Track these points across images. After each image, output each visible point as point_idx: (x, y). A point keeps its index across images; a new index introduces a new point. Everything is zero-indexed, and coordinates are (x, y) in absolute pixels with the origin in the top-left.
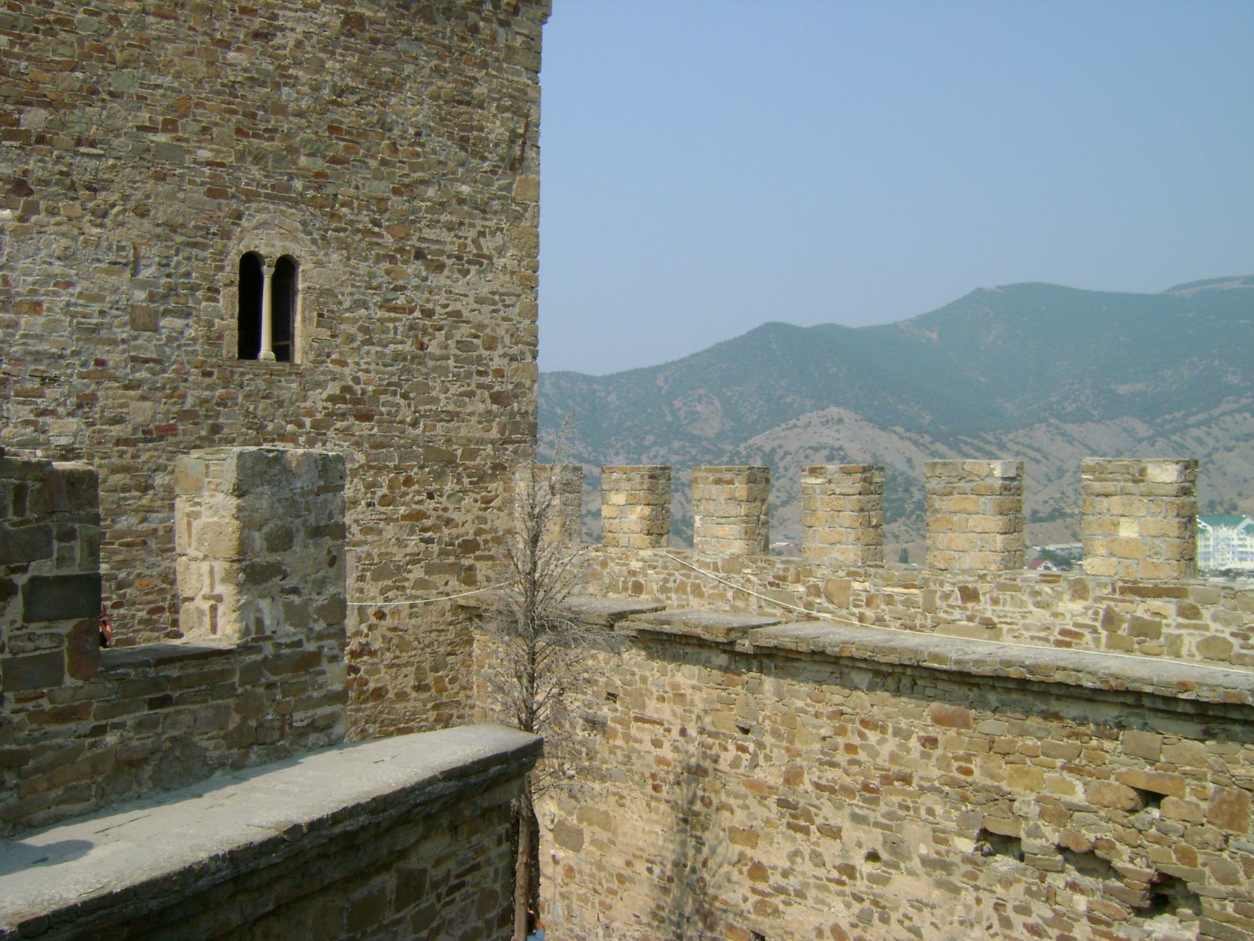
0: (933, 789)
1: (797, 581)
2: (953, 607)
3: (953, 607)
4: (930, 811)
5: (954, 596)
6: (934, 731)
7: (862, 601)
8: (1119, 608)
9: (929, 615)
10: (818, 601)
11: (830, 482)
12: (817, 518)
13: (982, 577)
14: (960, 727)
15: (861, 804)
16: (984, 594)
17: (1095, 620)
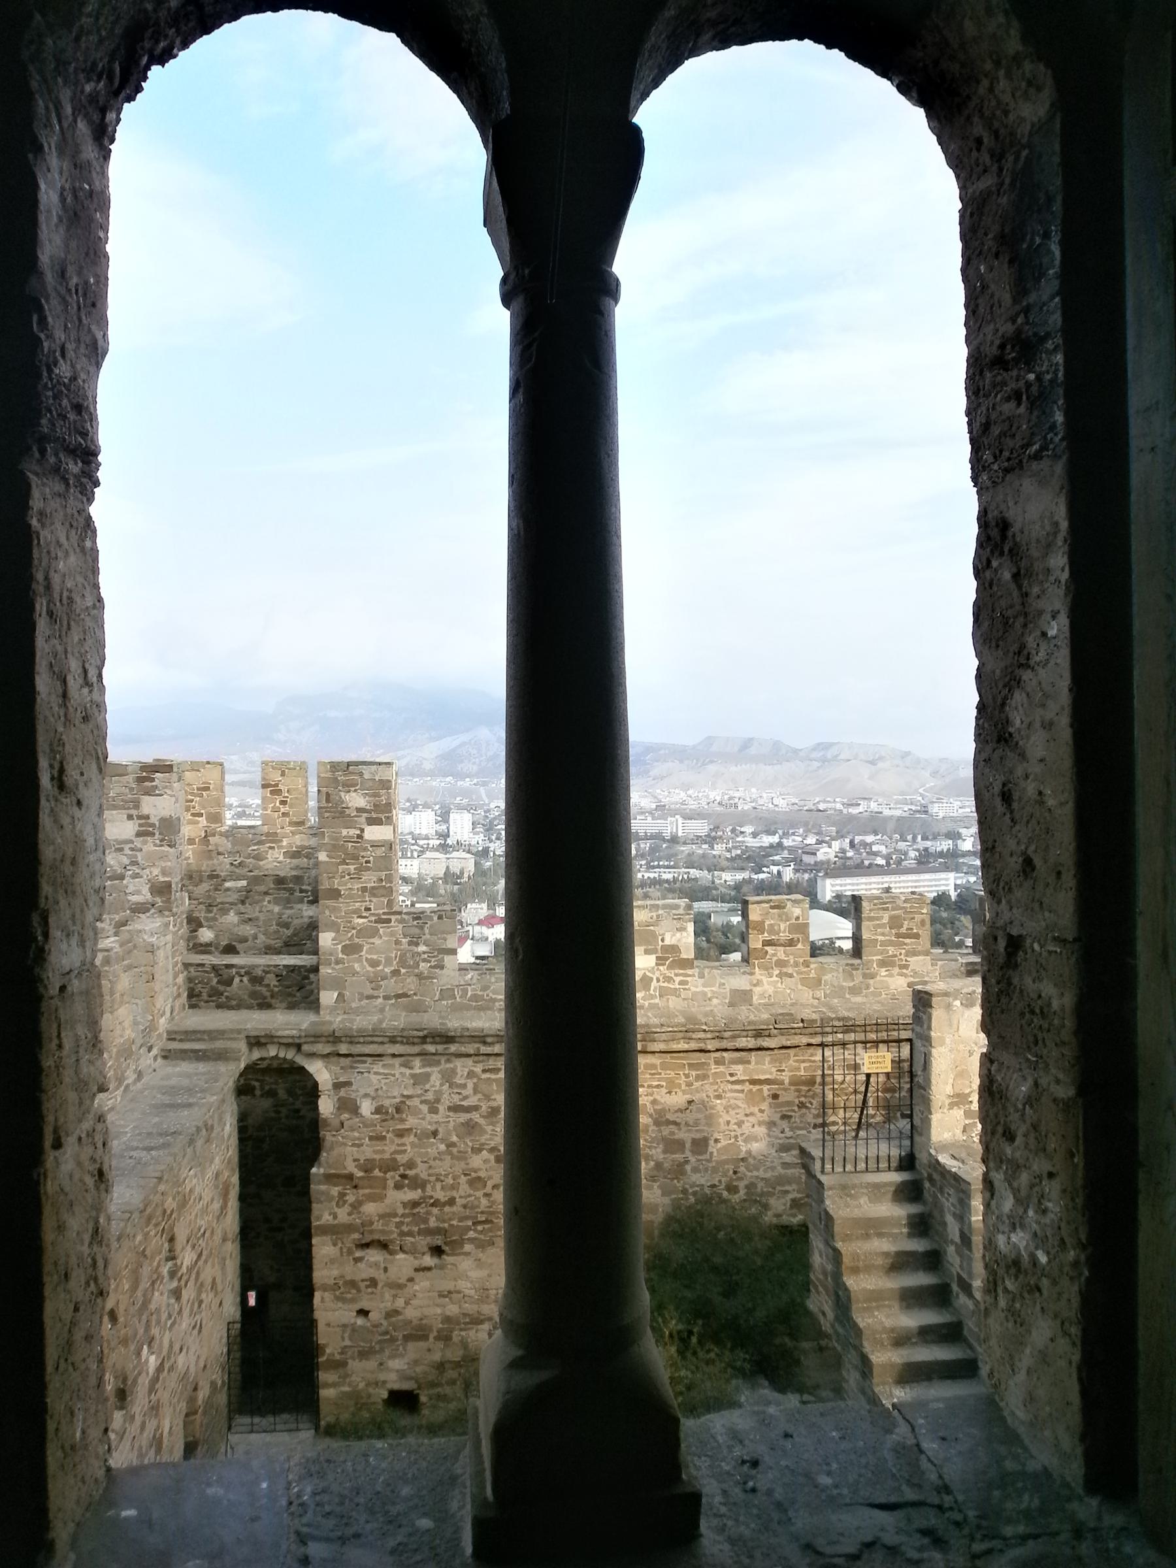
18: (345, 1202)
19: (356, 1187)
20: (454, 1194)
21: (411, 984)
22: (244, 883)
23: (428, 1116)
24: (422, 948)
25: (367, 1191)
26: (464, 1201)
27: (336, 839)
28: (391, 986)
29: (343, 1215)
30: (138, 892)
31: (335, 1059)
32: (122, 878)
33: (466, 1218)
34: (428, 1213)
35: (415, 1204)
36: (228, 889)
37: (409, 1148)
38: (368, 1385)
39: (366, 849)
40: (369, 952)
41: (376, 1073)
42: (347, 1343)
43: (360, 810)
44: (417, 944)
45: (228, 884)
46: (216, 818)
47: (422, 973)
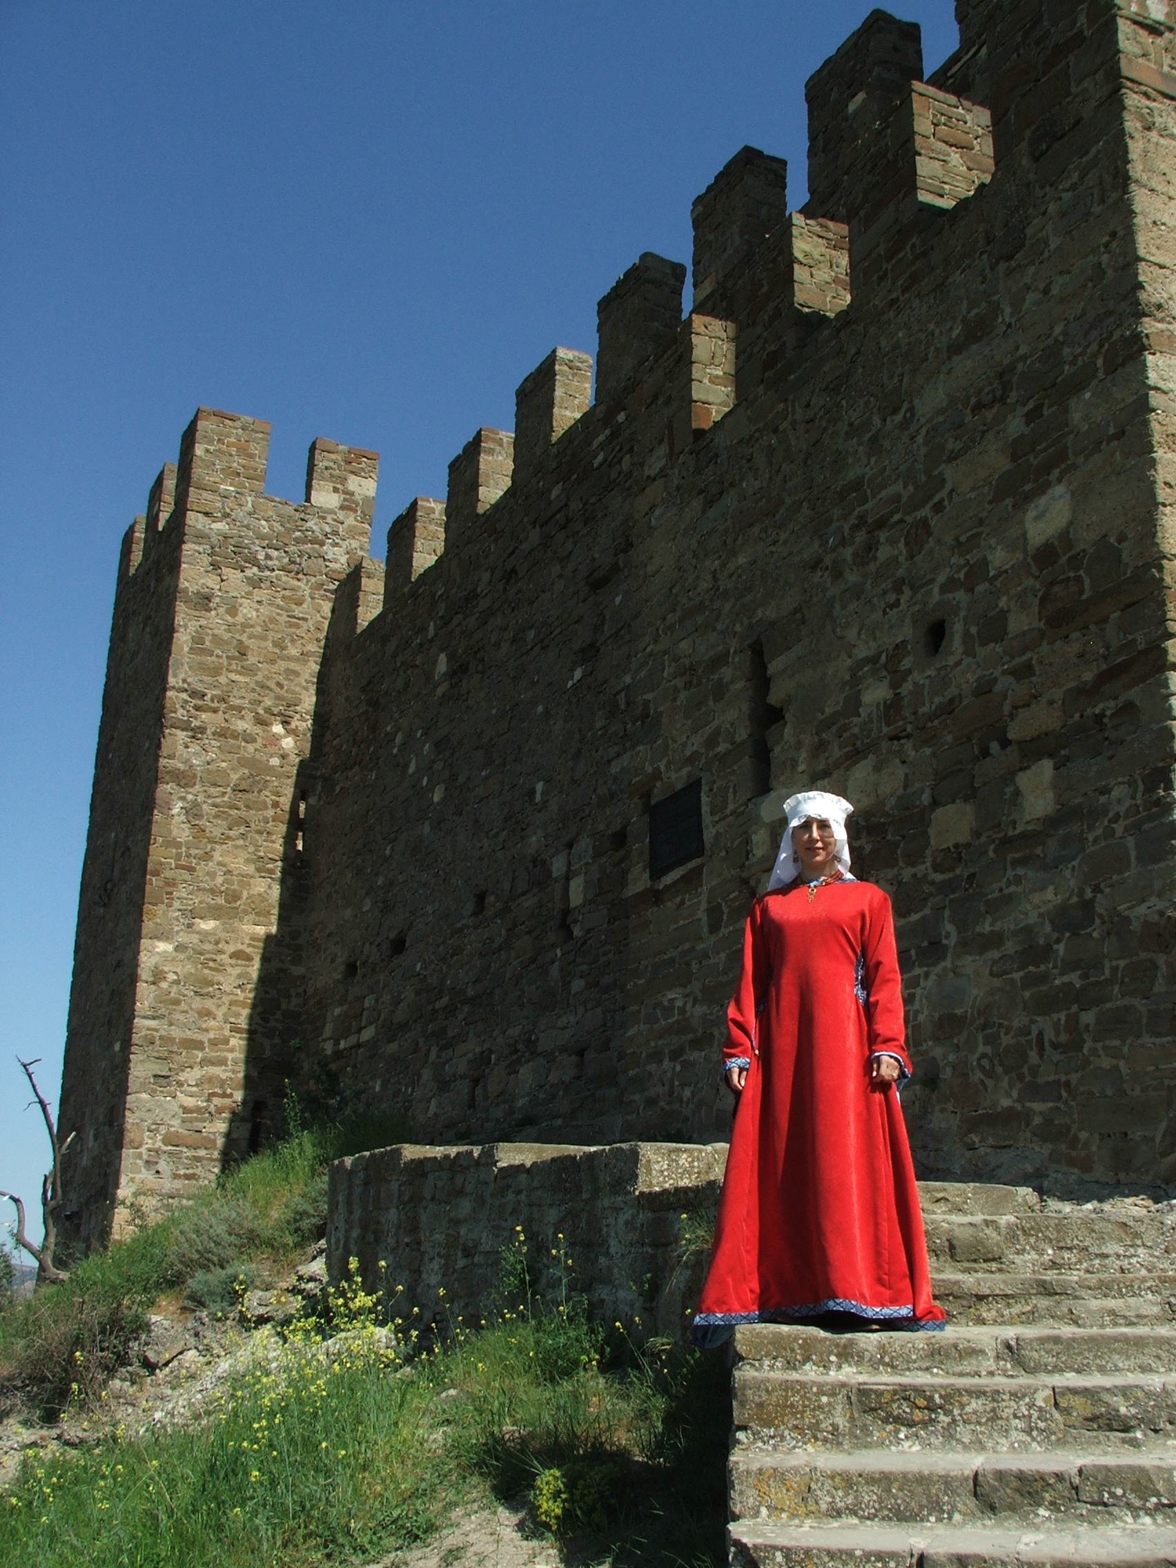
32: (322, 544)
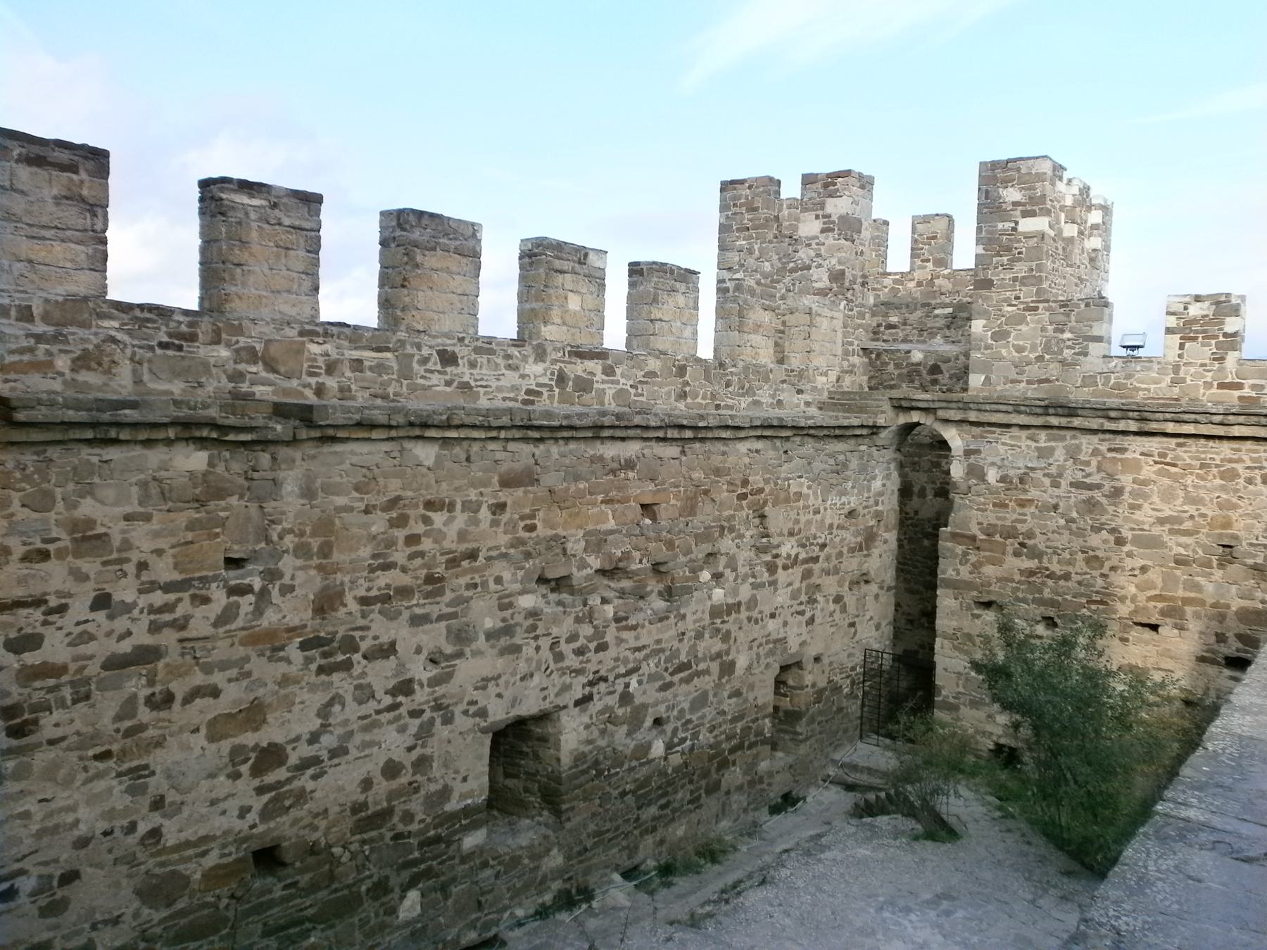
0: (504, 556)
1: (216, 341)
2: (432, 372)
3: (432, 372)
4: (498, 580)
5: (433, 360)
6: (503, 496)
7: (320, 368)
8: (568, 369)
9: (405, 382)
10: (254, 369)
11: (274, 206)
12: (251, 254)
13: (461, 340)
14: (526, 485)
15: (422, 601)
16: (462, 358)
17: (551, 379)
18: (967, 561)
19: (978, 548)
20: (1070, 569)
21: (1054, 370)
22: (950, 310)
23: (1050, 490)
24: (1067, 335)
25: (988, 554)
26: (1079, 578)
27: (991, 233)
28: (1034, 371)
29: (965, 573)
30: (820, 280)
31: (967, 427)
32: (809, 268)
33: (1082, 595)
34: (1043, 584)
35: (1032, 573)
36: (937, 316)
37: (1029, 518)
38: (977, 732)
39: (1019, 241)
40: (1016, 338)
41: (1003, 444)
42: (962, 690)
43: (1015, 204)
44: (1062, 332)
45: (937, 312)
46: (942, 262)
47: (1065, 359)
